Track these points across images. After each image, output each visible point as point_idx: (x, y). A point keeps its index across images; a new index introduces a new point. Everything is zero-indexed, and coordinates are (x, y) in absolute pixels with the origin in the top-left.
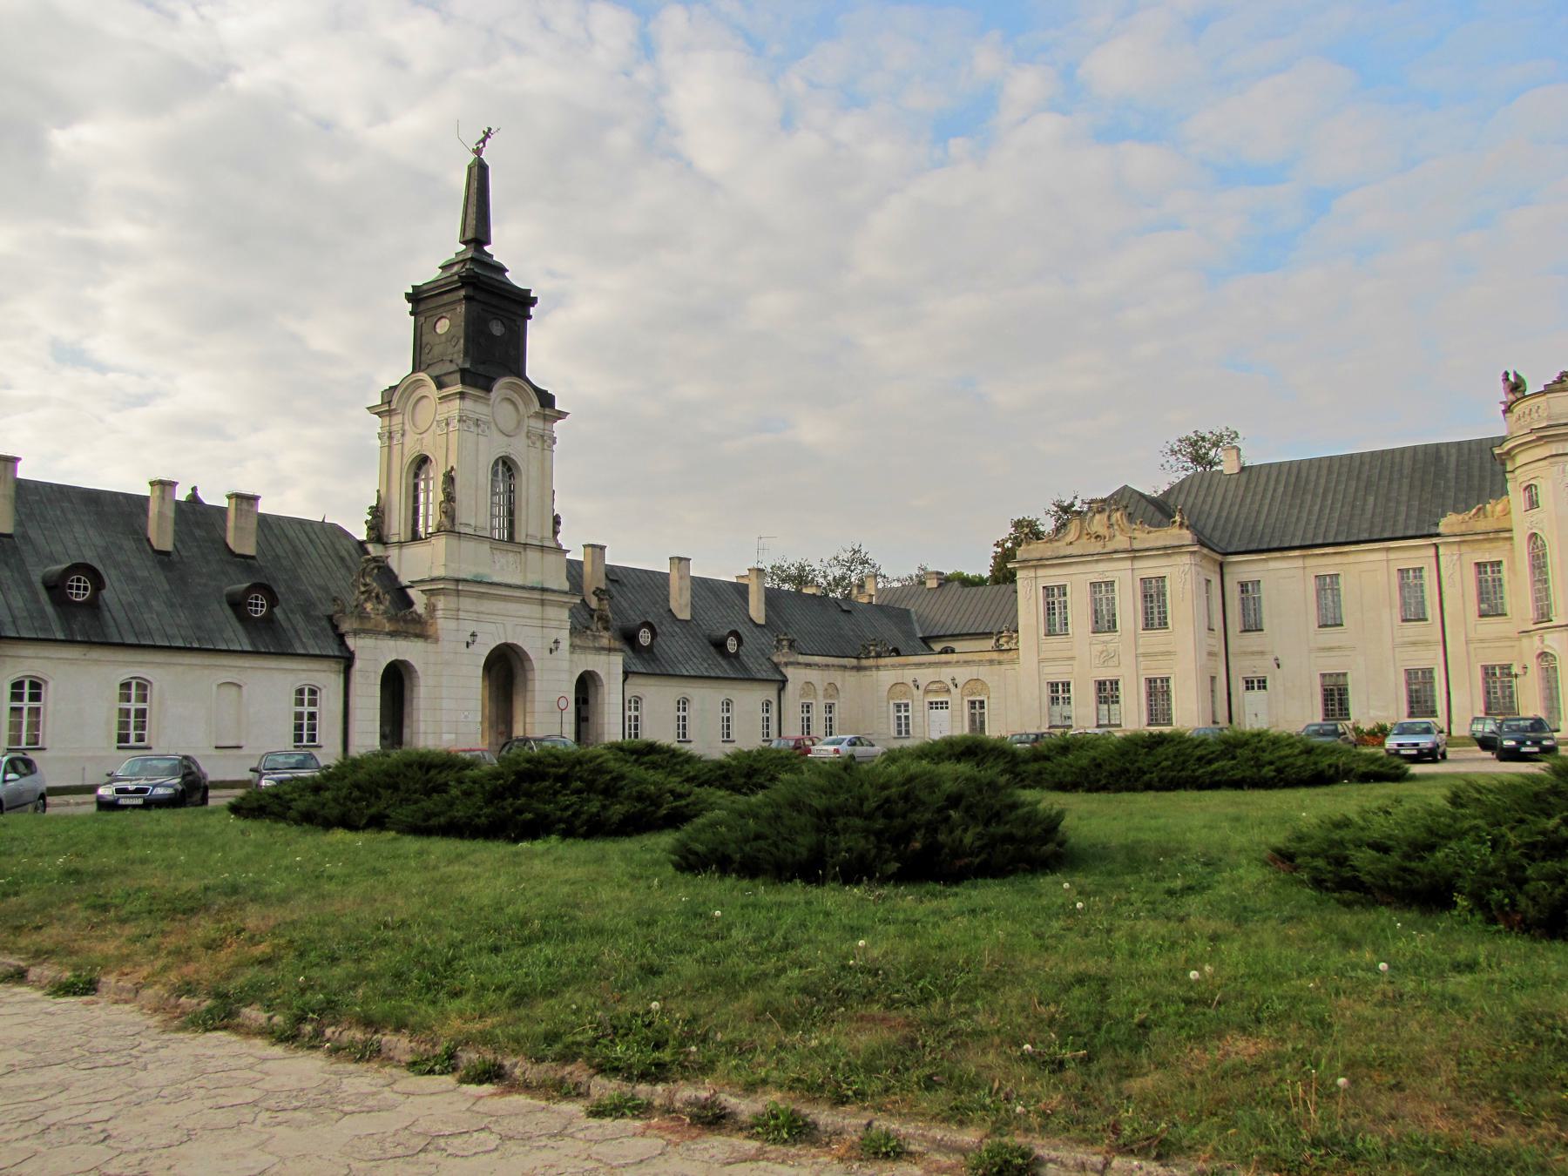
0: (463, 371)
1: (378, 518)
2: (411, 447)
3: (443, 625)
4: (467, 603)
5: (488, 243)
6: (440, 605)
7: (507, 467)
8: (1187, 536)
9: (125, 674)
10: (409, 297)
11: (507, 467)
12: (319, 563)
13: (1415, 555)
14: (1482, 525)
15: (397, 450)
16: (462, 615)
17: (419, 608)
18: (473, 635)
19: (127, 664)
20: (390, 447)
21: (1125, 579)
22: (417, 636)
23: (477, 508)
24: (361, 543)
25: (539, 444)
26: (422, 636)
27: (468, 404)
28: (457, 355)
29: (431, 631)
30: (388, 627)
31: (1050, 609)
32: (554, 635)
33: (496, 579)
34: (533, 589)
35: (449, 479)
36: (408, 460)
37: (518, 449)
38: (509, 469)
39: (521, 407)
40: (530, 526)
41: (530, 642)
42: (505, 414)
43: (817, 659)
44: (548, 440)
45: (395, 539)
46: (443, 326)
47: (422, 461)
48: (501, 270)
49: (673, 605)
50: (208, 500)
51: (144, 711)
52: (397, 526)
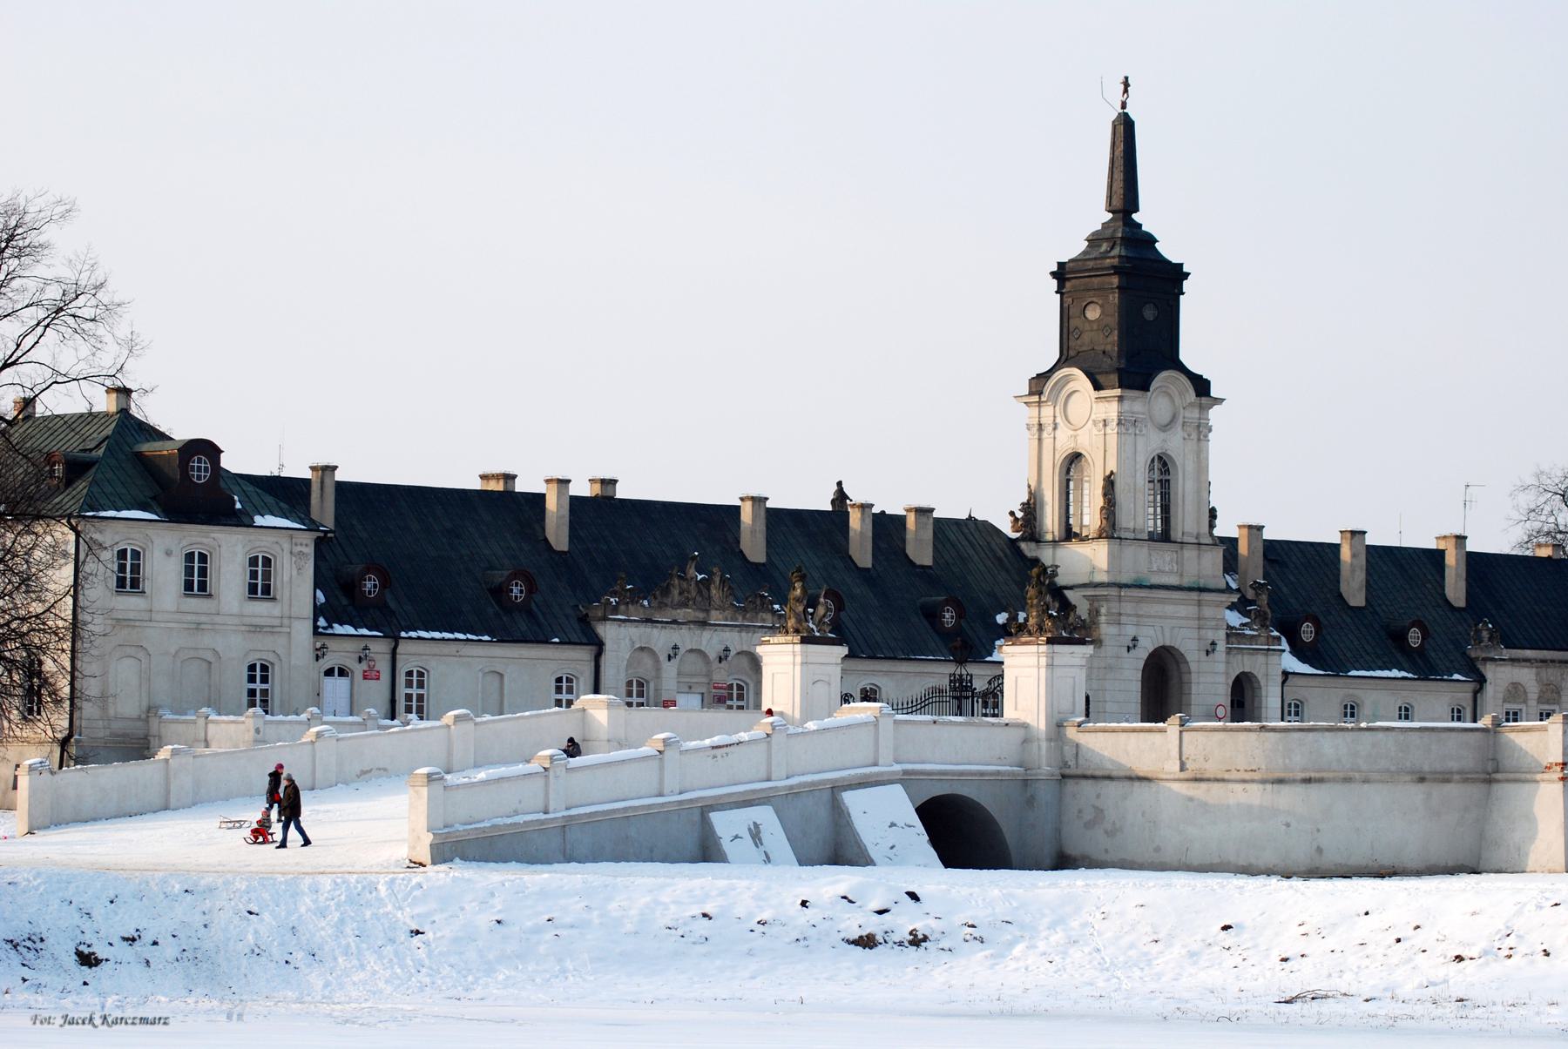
0: (1119, 371)
1: (1030, 515)
2: (1064, 442)
3: (1106, 630)
4: (1128, 608)
5: (1137, 210)
6: (1103, 610)
7: (1163, 465)
10: (1054, 274)
11: (1163, 465)
12: (983, 568)
15: (1047, 442)
16: (1124, 619)
17: (1083, 610)
18: (1135, 639)
19: (866, 672)
20: (1040, 439)
23: (1140, 514)
24: (1013, 542)
25: (1194, 436)
27: (1127, 405)
28: (1111, 342)
32: (1210, 635)
33: (1155, 580)
34: (1190, 589)
35: (1109, 483)
36: (1061, 455)
37: (1175, 444)
38: (1165, 464)
39: (1177, 400)
40: (1186, 522)
41: (1188, 644)
43: (1529, 653)
44: (1202, 431)
45: (1049, 537)
46: (1093, 313)
47: (1075, 458)
48: (1150, 240)
49: (1344, 588)
52: (1050, 522)
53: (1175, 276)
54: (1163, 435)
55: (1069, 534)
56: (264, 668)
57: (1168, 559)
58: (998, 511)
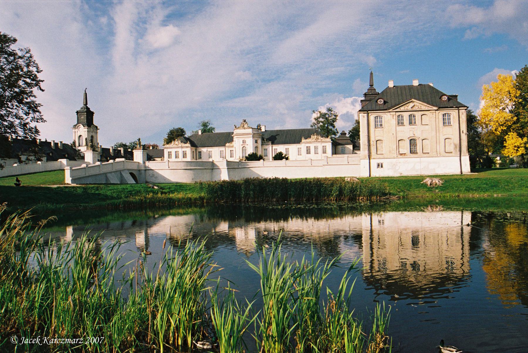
7: (92, 137)
8: (190, 145)
11: (92, 137)
13: (222, 149)
14: (231, 145)
21: (180, 151)
31: (169, 155)
35: (86, 139)
37: (94, 134)
44: (97, 133)
46: (82, 117)
47: (80, 136)
50: (48, 141)
52: (77, 144)
55: (79, 146)
58: (69, 142)
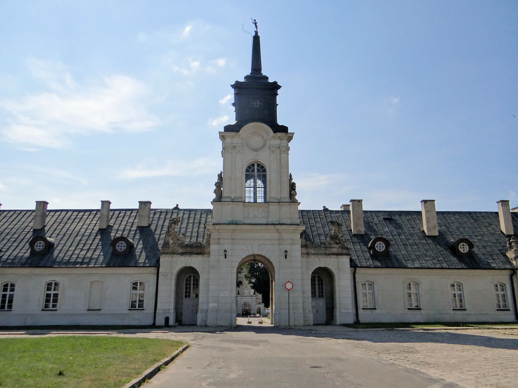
9: (49, 279)
19: (49, 275)
22: (197, 254)
26: (201, 253)
29: (207, 250)
30: (180, 251)
38: (262, 167)
41: (271, 252)
42: (256, 141)
51: (13, 295)
53: (275, 87)
54: (255, 153)
56: (12, 285)
57: (261, 211)
